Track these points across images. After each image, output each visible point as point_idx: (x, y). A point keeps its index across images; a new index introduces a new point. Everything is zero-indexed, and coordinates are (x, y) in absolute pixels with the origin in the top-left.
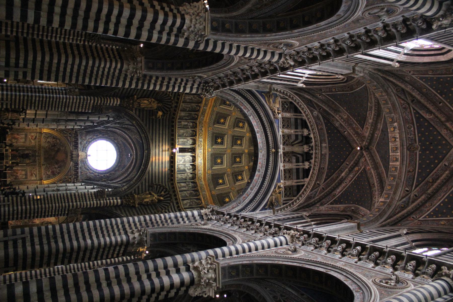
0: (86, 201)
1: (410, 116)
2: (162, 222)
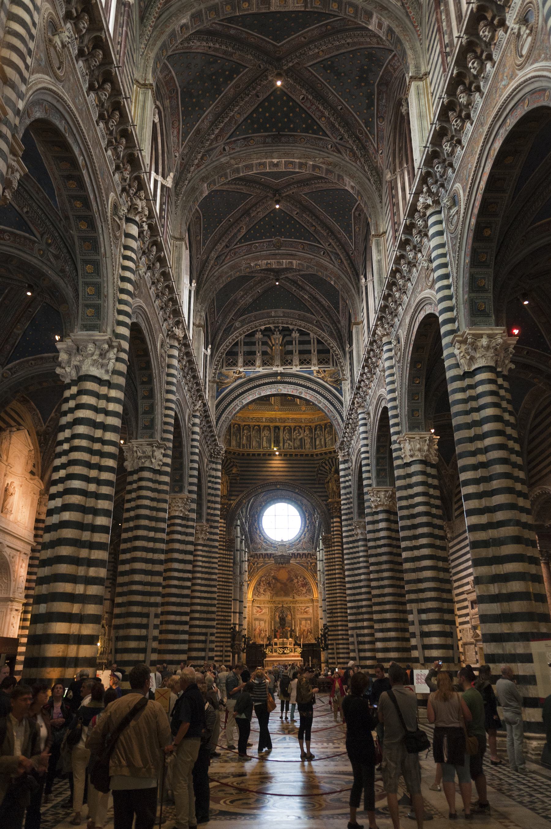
0: (334, 558)
1: (244, 248)
2: (349, 503)
